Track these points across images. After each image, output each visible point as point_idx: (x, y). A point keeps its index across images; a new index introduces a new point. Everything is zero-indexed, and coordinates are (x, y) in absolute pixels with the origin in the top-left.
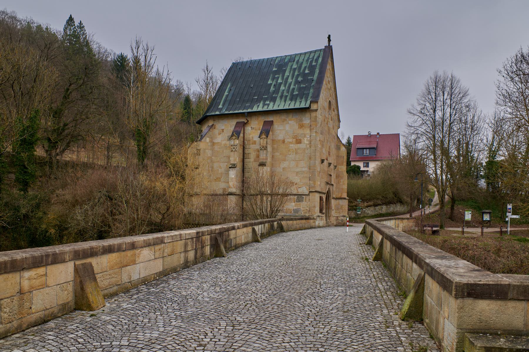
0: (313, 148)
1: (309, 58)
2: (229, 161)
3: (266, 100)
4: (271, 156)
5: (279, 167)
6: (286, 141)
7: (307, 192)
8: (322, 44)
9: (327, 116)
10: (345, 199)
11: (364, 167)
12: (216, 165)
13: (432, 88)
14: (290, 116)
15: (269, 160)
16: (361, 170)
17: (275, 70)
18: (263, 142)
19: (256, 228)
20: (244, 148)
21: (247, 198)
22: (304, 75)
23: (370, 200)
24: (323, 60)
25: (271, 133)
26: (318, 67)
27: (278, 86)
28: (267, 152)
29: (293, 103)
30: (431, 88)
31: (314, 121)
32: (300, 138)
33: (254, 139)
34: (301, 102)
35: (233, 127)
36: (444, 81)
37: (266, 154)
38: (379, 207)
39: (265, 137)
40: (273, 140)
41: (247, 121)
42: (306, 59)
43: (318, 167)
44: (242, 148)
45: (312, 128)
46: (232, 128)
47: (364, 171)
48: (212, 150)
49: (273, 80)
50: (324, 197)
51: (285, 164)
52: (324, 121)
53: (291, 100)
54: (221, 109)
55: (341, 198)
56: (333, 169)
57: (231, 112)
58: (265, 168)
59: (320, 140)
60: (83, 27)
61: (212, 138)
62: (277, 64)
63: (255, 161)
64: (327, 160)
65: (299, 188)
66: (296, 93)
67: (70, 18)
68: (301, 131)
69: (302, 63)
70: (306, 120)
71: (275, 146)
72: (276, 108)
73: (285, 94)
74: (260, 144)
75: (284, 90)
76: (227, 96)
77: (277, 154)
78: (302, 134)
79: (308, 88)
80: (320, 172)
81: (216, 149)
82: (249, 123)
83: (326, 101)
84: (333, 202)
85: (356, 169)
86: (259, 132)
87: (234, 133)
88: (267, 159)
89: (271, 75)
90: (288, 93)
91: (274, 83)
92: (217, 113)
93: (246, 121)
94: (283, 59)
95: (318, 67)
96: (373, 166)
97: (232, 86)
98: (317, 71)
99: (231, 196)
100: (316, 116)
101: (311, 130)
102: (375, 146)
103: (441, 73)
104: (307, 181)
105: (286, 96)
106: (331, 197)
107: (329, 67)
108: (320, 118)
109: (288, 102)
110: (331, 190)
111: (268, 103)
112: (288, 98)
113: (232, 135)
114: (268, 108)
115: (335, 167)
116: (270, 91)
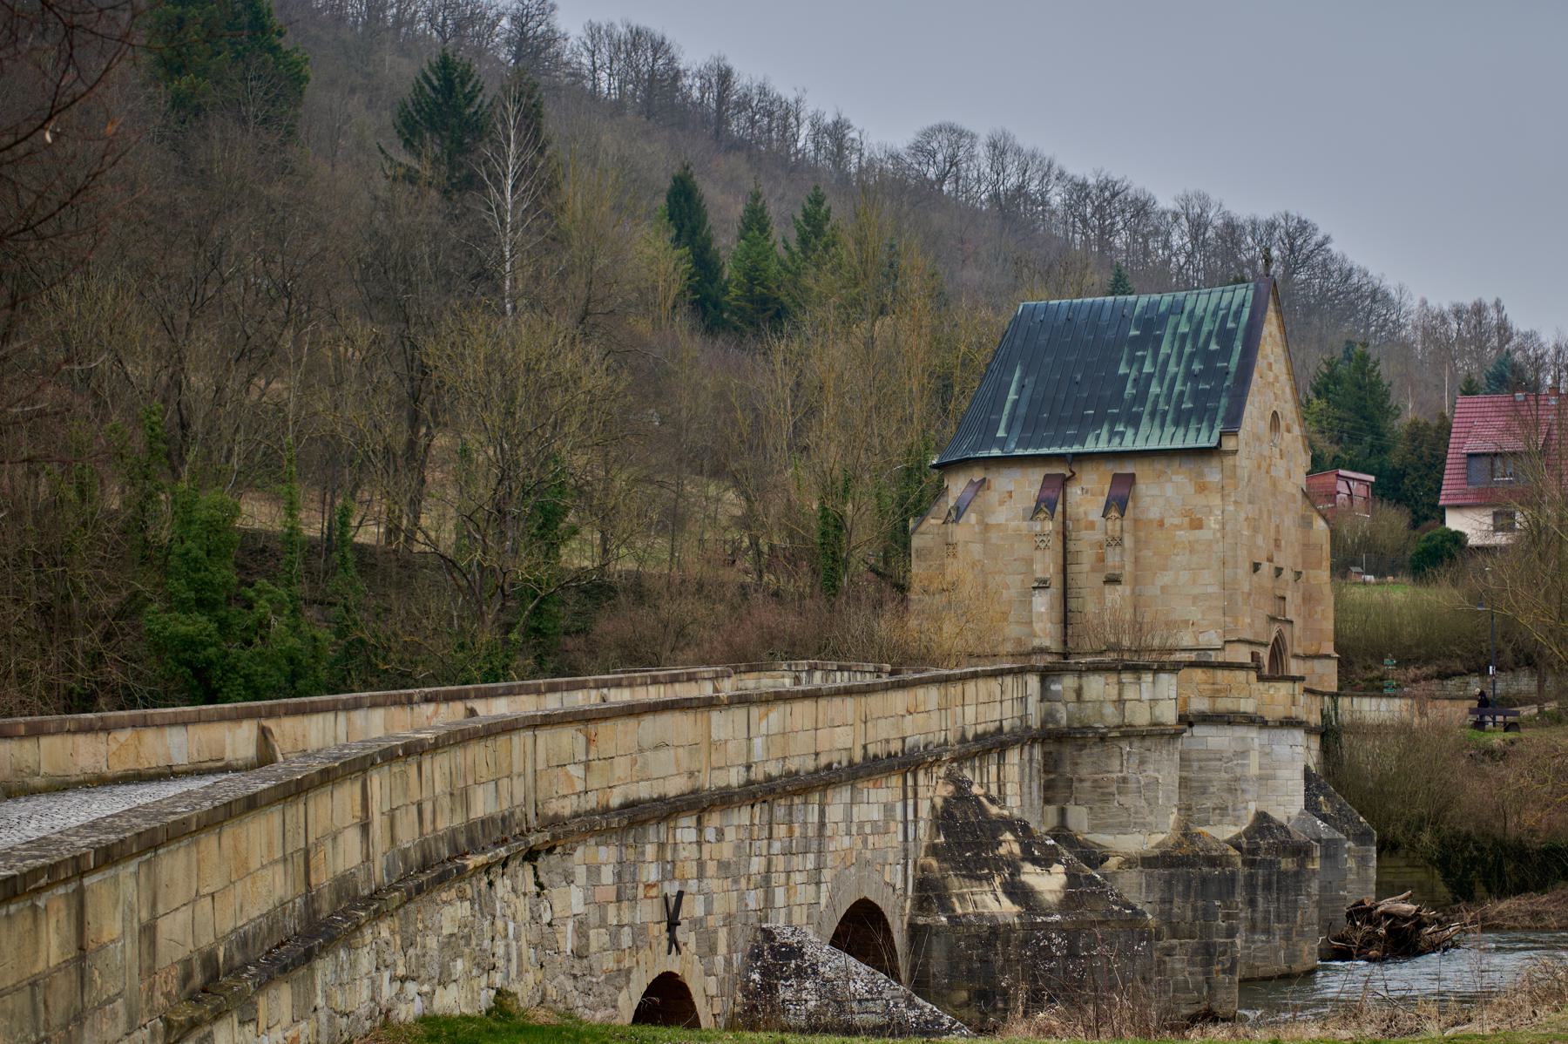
2: (1033, 572)
3: (1114, 420)
4: (1132, 559)
6: (1167, 522)
7: (1218, 643)
10: (1328, 657)
14: (1176, 463)
15: (1128, 568)
16: (1470, 542)
17: (1135, 336)
18: (1114, 526)
20: (1065, 537)
22: (1208, 357)
23: (1428, 660)
25: (1130, 504)
26: (1240, 335)
27: (1143, 383)
28: (1123, 550)
29: (1181, 431)
34: (1199, 430)
37: (1122, 556)
38: (1456, 681)
40: (1136, 521)
42: (1211, 307)
44: (1061, 538)
46: (1035, 490)
48: (985, 542)
49: (1130, 366)
51: (1165, 578)
52: (1259, 467)
53: (1176, 423)
54: (1002, 443)
55: (1318, 657)
56: (1291, 582)
57: (1030, 452)
58: (1119, 588)
61: (982, 514)
63: (1093, 570)
64: (1270, 560)
66: (1187, 405)
68: (1200, 500)
69: (1202, 318)
70: (1213, 473)
71: (1142, 534)
72: (1140, 445)
73: (1162, 406)
75: (1158, 396)
76: (1016, 403)
77: (1147, 553)
79: (1214, 394)
81: (994, 540)
83: (1263, 418)
86: (1102, 500)
87: (1042, 506)
88: (1123, 567)
89: (1126, 350)
90: (1168, 403)
92: (996, 452)
93: (1068, 474)
98: (1238, 346)
100: (1235, 466)
105: (1165, 414)
109: (1169, 429)
110: (1287, 635)
111: (1121, 429)
112: (1169, 418)
113: (1037, 510)
115: (1299, 574)
116: (1126, 396)
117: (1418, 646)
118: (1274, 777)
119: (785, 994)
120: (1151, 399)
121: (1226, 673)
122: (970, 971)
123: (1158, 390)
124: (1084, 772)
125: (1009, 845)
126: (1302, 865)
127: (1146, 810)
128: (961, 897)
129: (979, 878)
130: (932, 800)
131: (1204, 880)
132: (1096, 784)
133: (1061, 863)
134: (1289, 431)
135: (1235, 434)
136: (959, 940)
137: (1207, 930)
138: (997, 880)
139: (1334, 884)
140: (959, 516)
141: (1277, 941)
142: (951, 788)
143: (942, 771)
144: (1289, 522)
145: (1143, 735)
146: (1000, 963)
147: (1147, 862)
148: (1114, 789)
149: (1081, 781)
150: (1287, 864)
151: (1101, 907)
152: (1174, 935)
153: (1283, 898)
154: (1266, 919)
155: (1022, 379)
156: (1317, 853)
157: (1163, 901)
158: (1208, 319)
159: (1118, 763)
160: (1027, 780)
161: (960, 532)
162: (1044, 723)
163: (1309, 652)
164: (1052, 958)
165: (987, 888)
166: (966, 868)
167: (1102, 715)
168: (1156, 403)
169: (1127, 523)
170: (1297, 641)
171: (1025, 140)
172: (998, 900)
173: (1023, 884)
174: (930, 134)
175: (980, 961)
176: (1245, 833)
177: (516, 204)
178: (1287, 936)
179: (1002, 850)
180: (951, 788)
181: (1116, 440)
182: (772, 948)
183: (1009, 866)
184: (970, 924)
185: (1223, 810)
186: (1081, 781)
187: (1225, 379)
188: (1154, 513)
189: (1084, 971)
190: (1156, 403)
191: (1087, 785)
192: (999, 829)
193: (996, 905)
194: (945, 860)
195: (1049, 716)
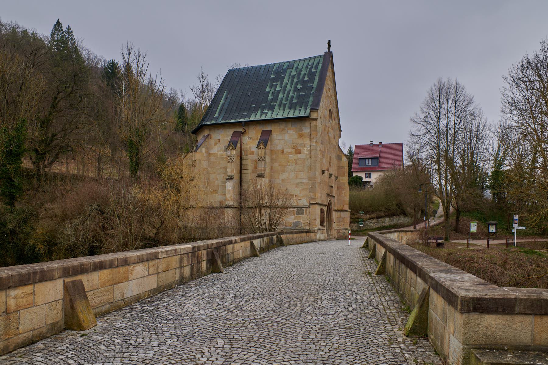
0: (313, 159)
1: (308, 65)
3: (264, 108)
5: (279, 178)
6: (285, 151)
7: (307, 204)
8: (322, 50)
9: (327, 125)
10: (346, 211)
11: (366, 178)
12: (212, 177)
13: (436, 96)
14: (289, 125)
15: (268, 171)
16: (363, 180)
17: (274, 77)
18: (261, 152)
19: (255, 242)
20: (241, 159)
21: (244, 211)
22: (303, 82)
23: (372, 212)
24: (322, 67)
25: (269, 143)
26: (318, 74)
28: (266, 162)
29: (292, 111)
30: (435, 95)
31: (314, 131)
32: (299, 148)
33: (252, 150)
34: (300, 110)
35: (230, 137)
36: (448, 88)
37: (265, 165)
38: (382, 219)
39: (263, 147)
40: (271, 151)
41: (244, 131)
42: (305, 65)
43: (319, 178)
45: (312, 137)
46: (229, 138)
47: (366, 182)
48: (208, 161)
49: (271, 87)
50: (325, 209)
51: (284, 176)
52: (325, 130)
53: (290, 108)
54: (217, 118)
55: (342, 211)
56: (334, 180)
57: (227, 121)
58: (263, 179)
59: (320, 150)
60: (72, 32)
61: (208, 149)
62: (275, 70)
63: (253, 172)
64: (328, 170)
65: (299, 200)
66: (295, 101)
67: (57, 22)
68: (300, 141)
69: (301, 69)
70: (306, 129)
71: (274, 156)
72: (274, 117)
73: (284, 102)
74: (258, 155)
75: (282, 98)
76: (223, 104)
77: (276, 165)
78: (302, 144)
79: (307, 96)
80: (320, 184)
82: (246, 133)
83: (327, 110)
84: (335, 215)
85: (358, 180)
86: (257, 142)
87: (231, 144)
88: (265, 170)
90: (287, 101)
91: (272, 91)
92: (213, 122)
93: (243, 131)
94: (281, 66)
95: (318, 74)
96: (375, 177)
98: (317, 78)
99: (229, 209)
100: (316, 125)
101: (310, 140)
102: (377, 156)
103: (445, 80)
105: (285, 105)
106: (333, 209)
107: (329, 74)
108: (320, 127)
109: (287, 111)
110: (332, 202)
111: (266, 111)
112: (287, 106)
113: (229, 146)
114: (266, 117)
115: (337, 178)
116: (268, 99)
123: (282, 96)
135: (317, 111)
155: (227, 95)
163: (339, 209)
187: (312, 90)
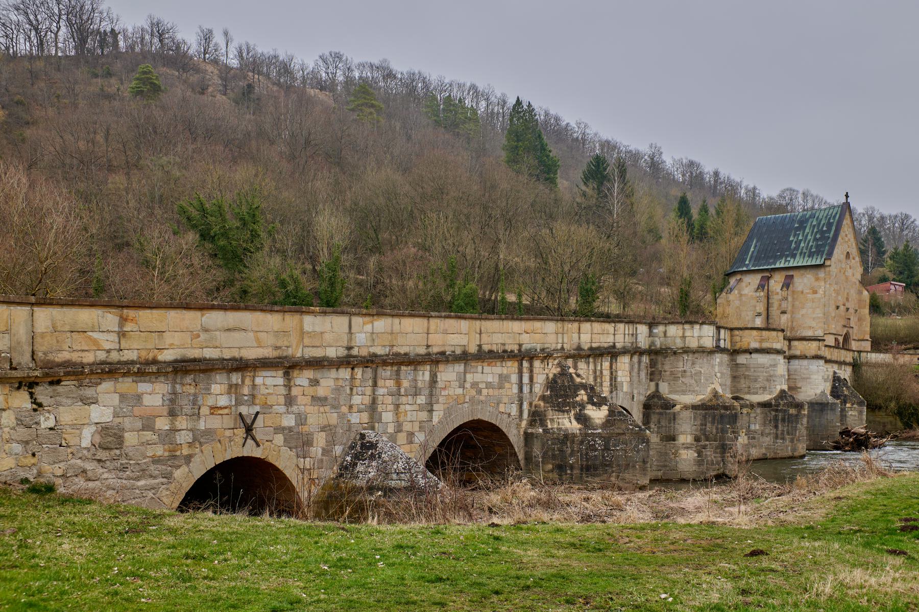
3: (787, 256)
6: (805, 291)
10: (867, 340)
12: (743, 314)
14: (808, 271)
15: (790, 308)
18: (785, 293)
22: (822, 232)
25: (791, 285)
26: (835, 224)
27: (798, 243)
29: (811, 259)
40: (793, 292)
46: (758, 282)
48: (740, 300)
49: (794, 237)
51: (803, 311)
53: (809, 256)
57: (757, 268)
63: (778, 309)
64: (844, 305)
66: (814, 250)
68: (817, 284)
70: (821, 273)
71: (795, 296)
72: (795, 265)
73: (804, 250)
76: (753, 252)
79: (823, 245)
86: (781, 284)
91: (795, 239)
92: (745, 269)
97: (757, 242)
104: (822, 325)
105: (805, 253)
109: (806, 258)
113: (758, 288)
115: (856, 310)
117: (906, 337)
118: (810, 378)
119: (360, 468)
120: (801, 248)
121: (767, 332)
122: (553, 455)
124: (667, 367)
125: (582, 396)
126: (799, 412)
127: (695, 385)
128: (552, 420)
129: (563, 412)
130: (547, 375)
131: (722, 416)
132: (672, 373)
133: (606, 405)
134: (854, 259)
135: (830, 259)
136: (548, 440)
137: (723, 439)
138: (573, 412)
139: (835, 420)
140: (731, 291)
141: (787, 443)
142: (559, 369)
143: (556, 362)
144: (853, 293)
145: (694, 352)
146: (569, 452)
147: (694, 407)
148: (680, 375)
149: (665, 371)
150: (792, 411)
151: (623, 426)
152: (707, 439)
153: (790, 425)
154: (782, 434)
156: (806, 407)
157: (702, 425)
158: (824, 219)
159: (682, 363)
160: (636, 370)
161: (731, 297)
162: (650, 346)
164: (596, 450)
165: (566, 416)
166: (558, 406)
167: (675, 343)
168: (802, 250)
169: (790, 292)
170: (854, 333)
171: (814, 192)
172: (571, 422)
173: (585, 415)
174: (784, 191)
175: (559, 451)
176: (774, 398)
177: (618, 202)
178: (792, 441)
179: (578, 399)
180: (559, 369)
181: (787, 263)
182: (362, 444)
183: (580, 405)
184: (554, 433)
185: (764, 388)
186: (665, 371)
188: (800, 288)
189: (613, 456)
190: (802, 250)
191: (668, 373)
192: (579, 388)
193: (569, 424)
194: (548, 403)
195: (653, 343)
